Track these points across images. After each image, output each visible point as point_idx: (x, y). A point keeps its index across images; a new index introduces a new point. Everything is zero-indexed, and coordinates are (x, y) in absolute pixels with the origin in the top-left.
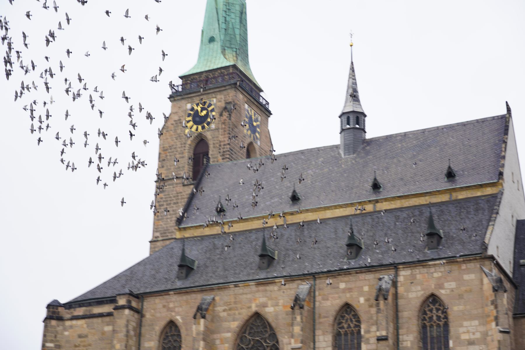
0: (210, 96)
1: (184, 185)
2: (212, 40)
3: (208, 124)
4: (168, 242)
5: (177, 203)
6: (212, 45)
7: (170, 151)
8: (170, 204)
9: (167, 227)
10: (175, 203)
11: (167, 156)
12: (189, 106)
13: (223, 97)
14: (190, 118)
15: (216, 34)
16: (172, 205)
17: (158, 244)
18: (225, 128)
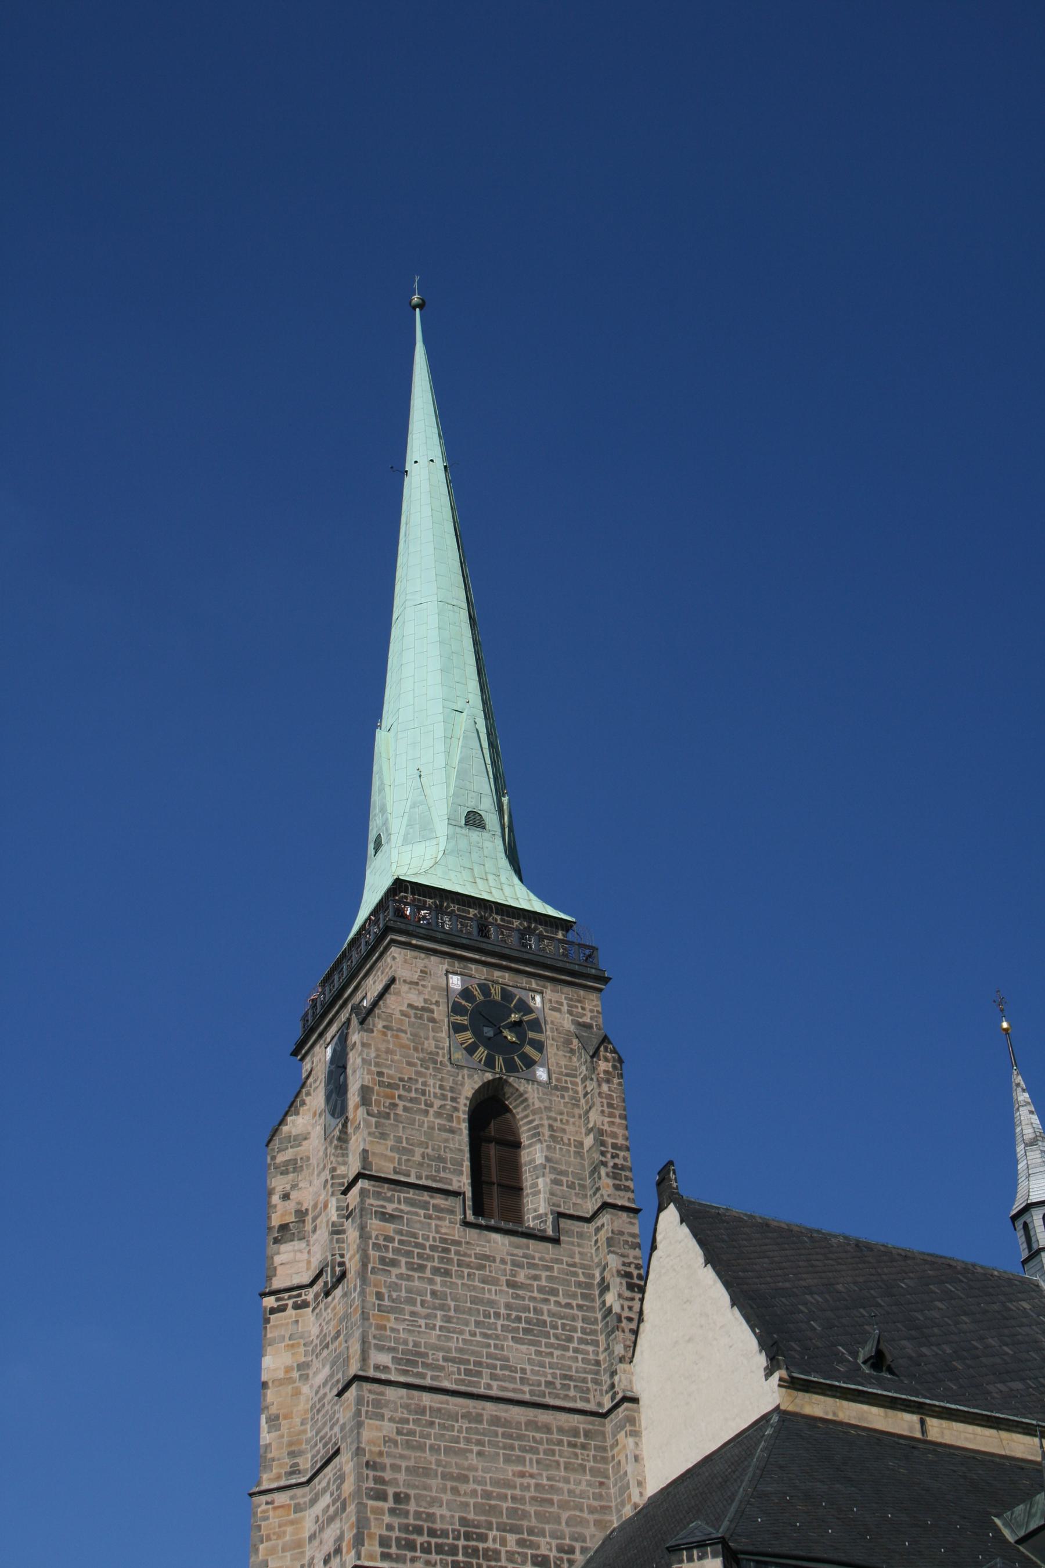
0: (523, 981)
1: (466, 1224)
2: (474, 820)
3: (530, 1063)
4: (427, 1399)
5: (447, 1273)
6: (475, 835)
7: (402, 1092)
8: (421, 1268)
9: (416, 1344)
10: (436, 1271)
11: (395, 1105)
12: (456, 982)
13: (563, 999)
14: (464, 1020)
15: (486, 806)
16: (428, 1274)
17: (391, 1393)
18: (610, 1097)
